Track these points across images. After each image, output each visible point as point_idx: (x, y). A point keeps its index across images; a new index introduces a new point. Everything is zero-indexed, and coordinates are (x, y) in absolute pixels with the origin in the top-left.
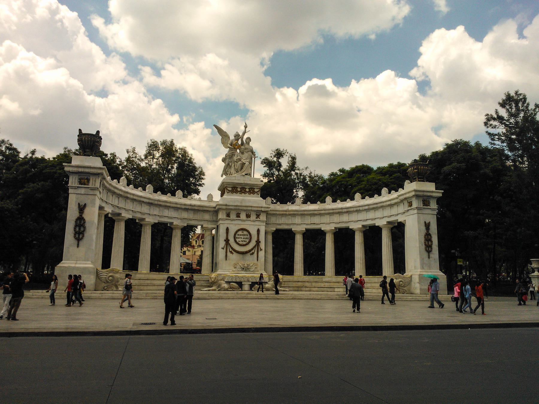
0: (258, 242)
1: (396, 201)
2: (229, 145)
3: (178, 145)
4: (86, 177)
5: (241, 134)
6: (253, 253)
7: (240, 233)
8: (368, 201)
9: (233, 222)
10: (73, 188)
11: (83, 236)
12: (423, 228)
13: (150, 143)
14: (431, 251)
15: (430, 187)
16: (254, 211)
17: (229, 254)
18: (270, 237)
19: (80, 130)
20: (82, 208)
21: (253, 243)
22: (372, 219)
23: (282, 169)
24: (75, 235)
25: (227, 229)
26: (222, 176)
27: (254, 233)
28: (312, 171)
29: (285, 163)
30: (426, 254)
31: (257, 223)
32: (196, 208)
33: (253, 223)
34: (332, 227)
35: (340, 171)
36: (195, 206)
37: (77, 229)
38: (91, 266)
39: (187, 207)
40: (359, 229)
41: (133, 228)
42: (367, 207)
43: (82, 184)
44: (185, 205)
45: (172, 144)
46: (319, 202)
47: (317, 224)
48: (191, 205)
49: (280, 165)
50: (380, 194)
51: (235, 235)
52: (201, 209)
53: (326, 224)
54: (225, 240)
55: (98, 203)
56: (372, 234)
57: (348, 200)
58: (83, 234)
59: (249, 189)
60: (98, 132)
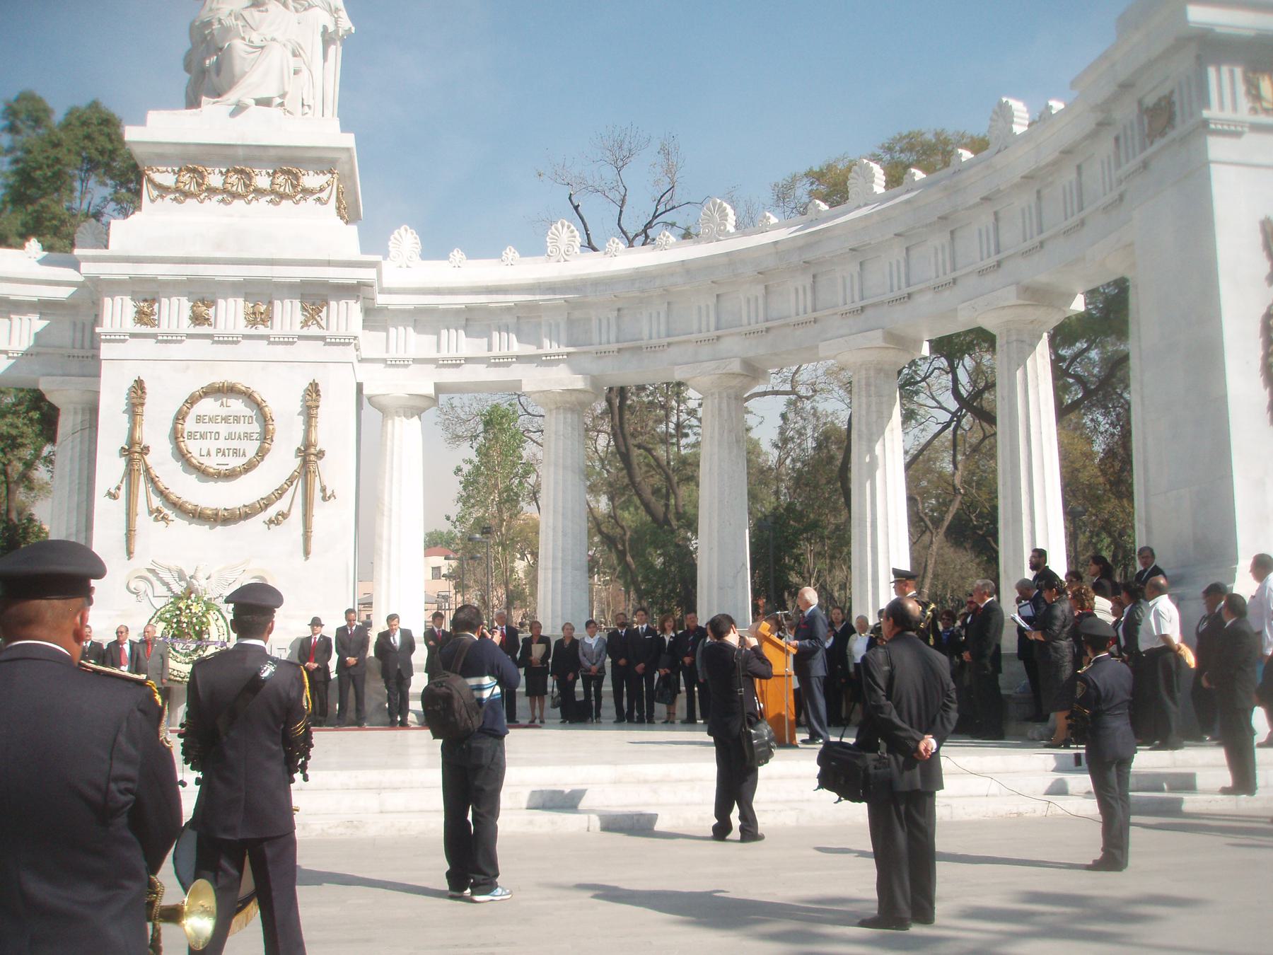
0: (308, 455)
7: (208, 406)
9: (173, 350)
17: (143, 520)
21: (282, 461)
33: (280, 351)
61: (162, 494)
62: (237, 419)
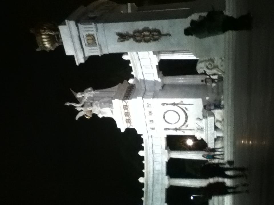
0: (174, 104)
6: (186, 109)
14: (158, 31)
17: (188, 128)
21: (176, 108)
25: (166, 129)
61: (183, 125)
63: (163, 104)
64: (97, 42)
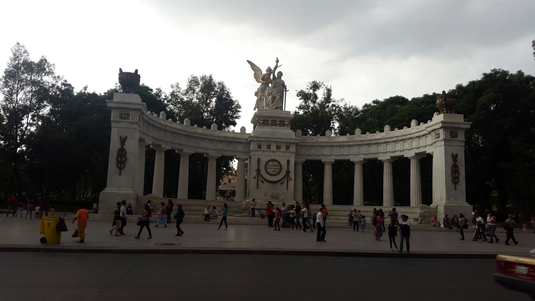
0: (288, 172)
1: (424, 132)
2: (260, 80)
3: (216, 80)
4: (126, 112)
5: (272, 68)
6: (283, 183)
7: (271, 163)
8: (397, 132)
9: (264, 153)
10: (114, 122)
11: (125, 165)
12: (451, 160)
13: (190, 78)
14: (458, 182)
15: (459, 118)
16: (284, 143)
17: (260, 183)
18: (300, 168)
19: (120, 69)
20: (123, 141)
22: (401, 151)
23: (318, 101)
24: (117, 164)
25: (259, 160)
26: (255, 109)
27: (284, 163)
28: (347, 102)
29: (321, 94)
30: (453, 185)
31: (287, 154)
32: (230, 140)
33: (282, 154)
34: (361, 158)
35: (374, 102)
36: (228, 138)
37: (119, 159)
38: (132, 192)
39: (221, 139)
40: (388, 160)
41: (172, 159)
42: (395, 139)
43: (122, 119)
44: (219, 137)
45: (211, 79)
46: (348, 134)
47: (346, 155)
48: (225, 137)
49: (316, 97)
50: (409, 126)
51: (266, 165)
52: (235, 140)
53: (355, 155)
54: (256, 170)
55: (138, 135)
56: (400, 165)
57: (377, 132)
58: (125, 164)
59: (280, 121)
60: (137, 71)
62: (275, 166)
63: (288, 162)
64: (453, 139)
